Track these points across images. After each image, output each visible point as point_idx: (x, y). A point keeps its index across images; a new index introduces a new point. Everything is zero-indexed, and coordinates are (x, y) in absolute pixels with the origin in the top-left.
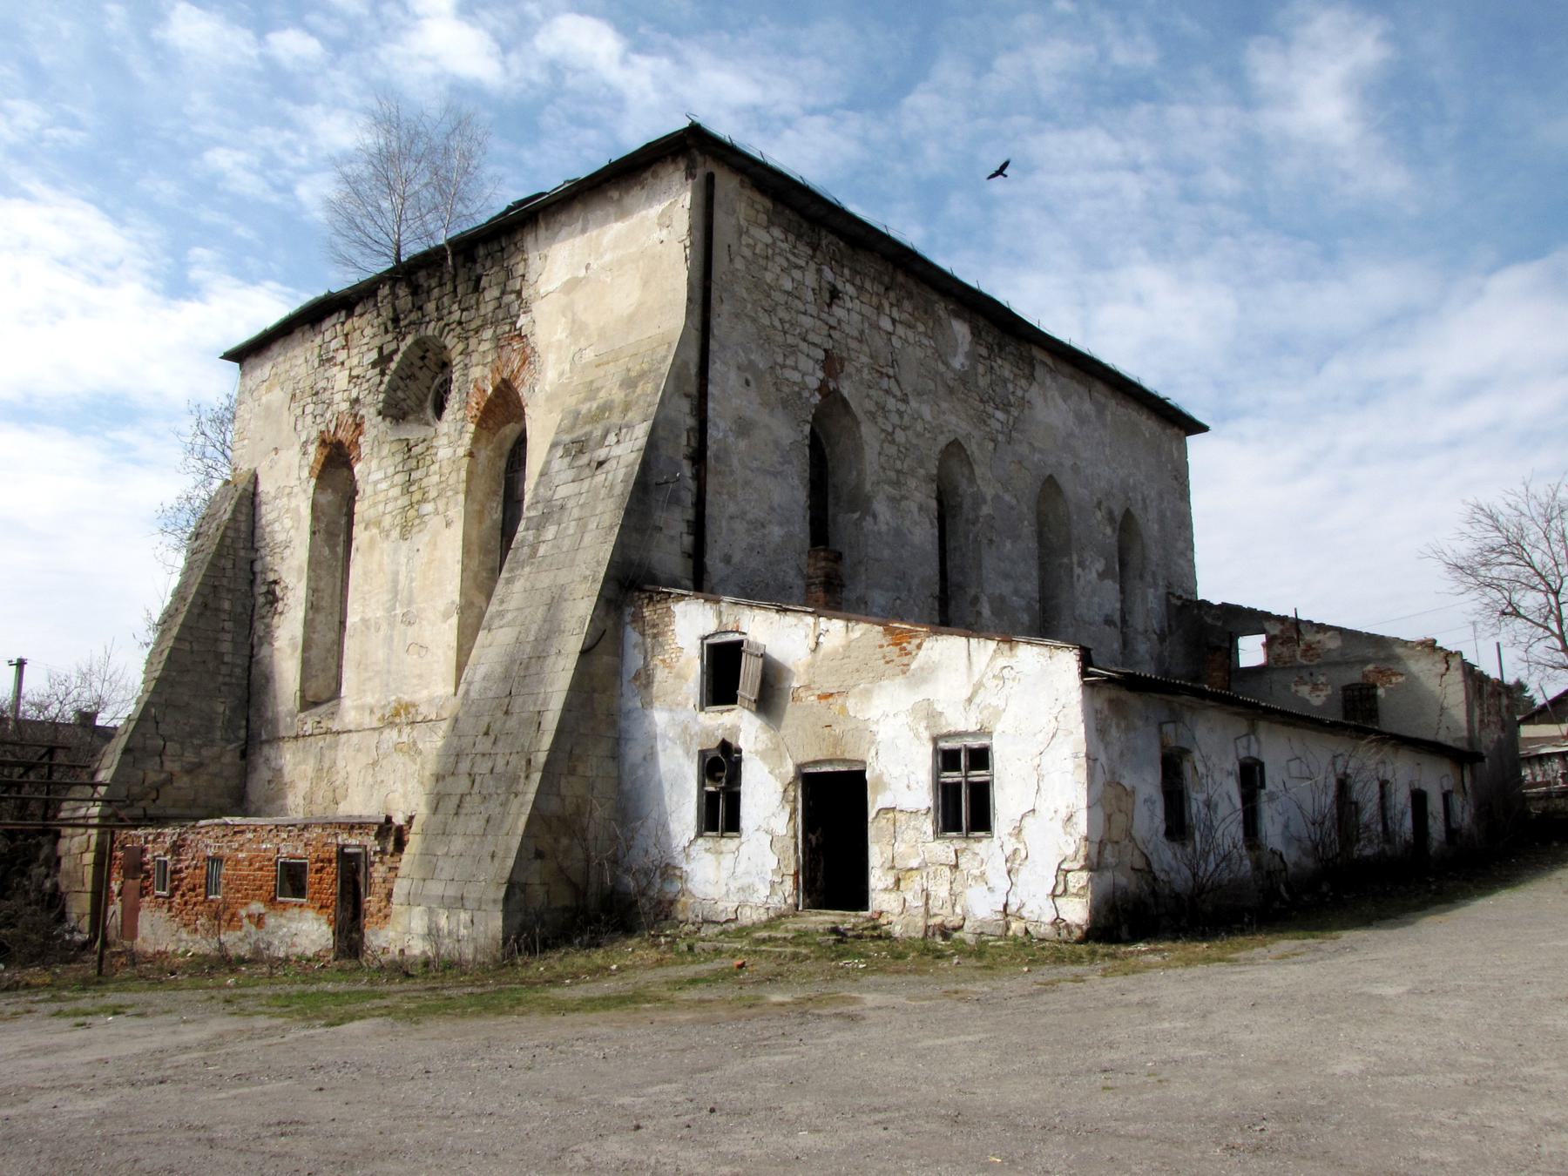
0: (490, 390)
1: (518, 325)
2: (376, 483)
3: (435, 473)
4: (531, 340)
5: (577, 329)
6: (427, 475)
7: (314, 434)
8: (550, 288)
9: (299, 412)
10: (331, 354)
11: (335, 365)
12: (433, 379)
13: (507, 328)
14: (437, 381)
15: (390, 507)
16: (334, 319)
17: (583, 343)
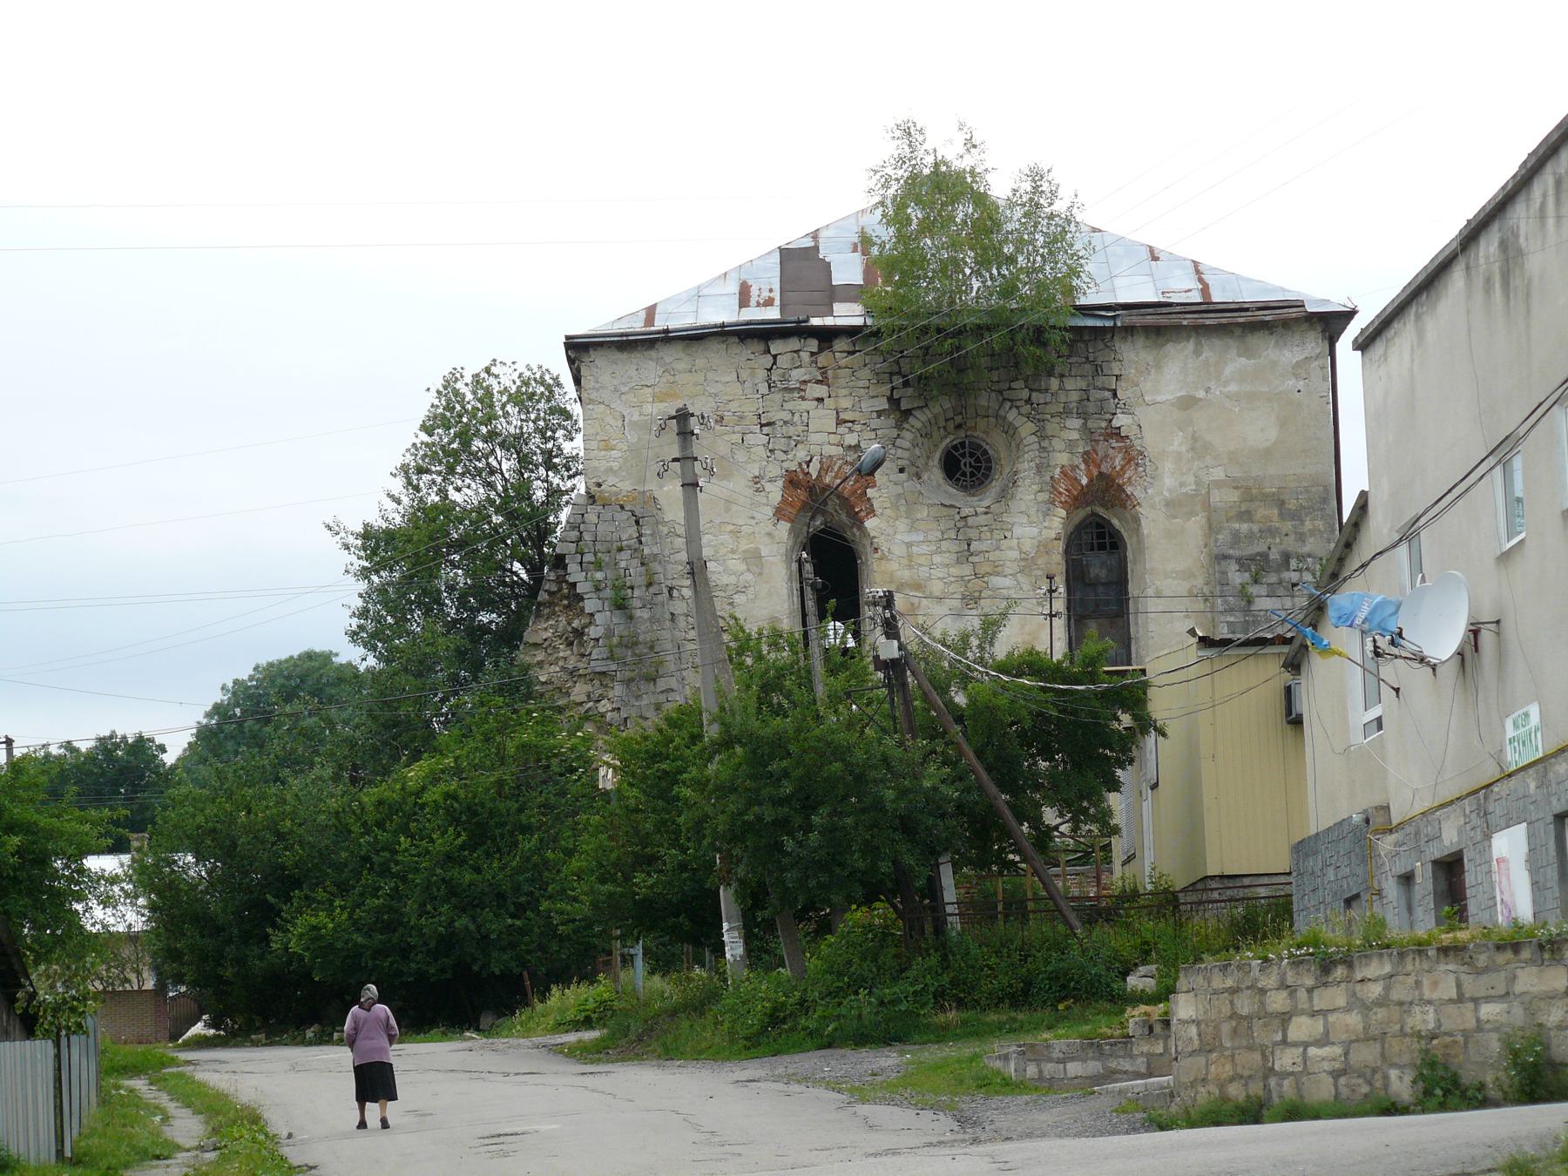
0: (1084, 481)
1: (1116, 423)
2: (909, 545)
3: (1011, 548)
4: (1137, 442)
5: (1198, 447)
6: (998, 548)
7: (775, 470)
8: (1159, 399)
9: (737, 438)
10: (793, 384)
11: (803, 398)
12: (946, 437)
13: (1104, 424)
14: (943, 445)
15: (937, 573)
16: (794, 343)
17: (1209, 460)
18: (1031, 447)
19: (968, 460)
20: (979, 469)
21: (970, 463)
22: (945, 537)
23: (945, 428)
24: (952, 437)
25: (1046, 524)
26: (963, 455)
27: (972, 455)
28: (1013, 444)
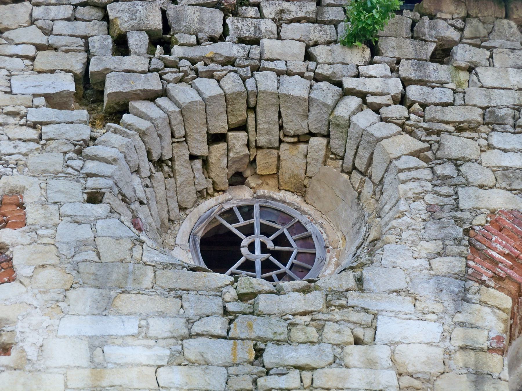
12: (202, 195)
18: (413, 174)
19: (258, 239)
20: (283, 257)
21: (263, 246)
22: (197, 328)
23: (205, 162)
24: (220, 197)
25: (460, 318)
26: (248, 231)
27: (266, 231)
28: (368, 189)
